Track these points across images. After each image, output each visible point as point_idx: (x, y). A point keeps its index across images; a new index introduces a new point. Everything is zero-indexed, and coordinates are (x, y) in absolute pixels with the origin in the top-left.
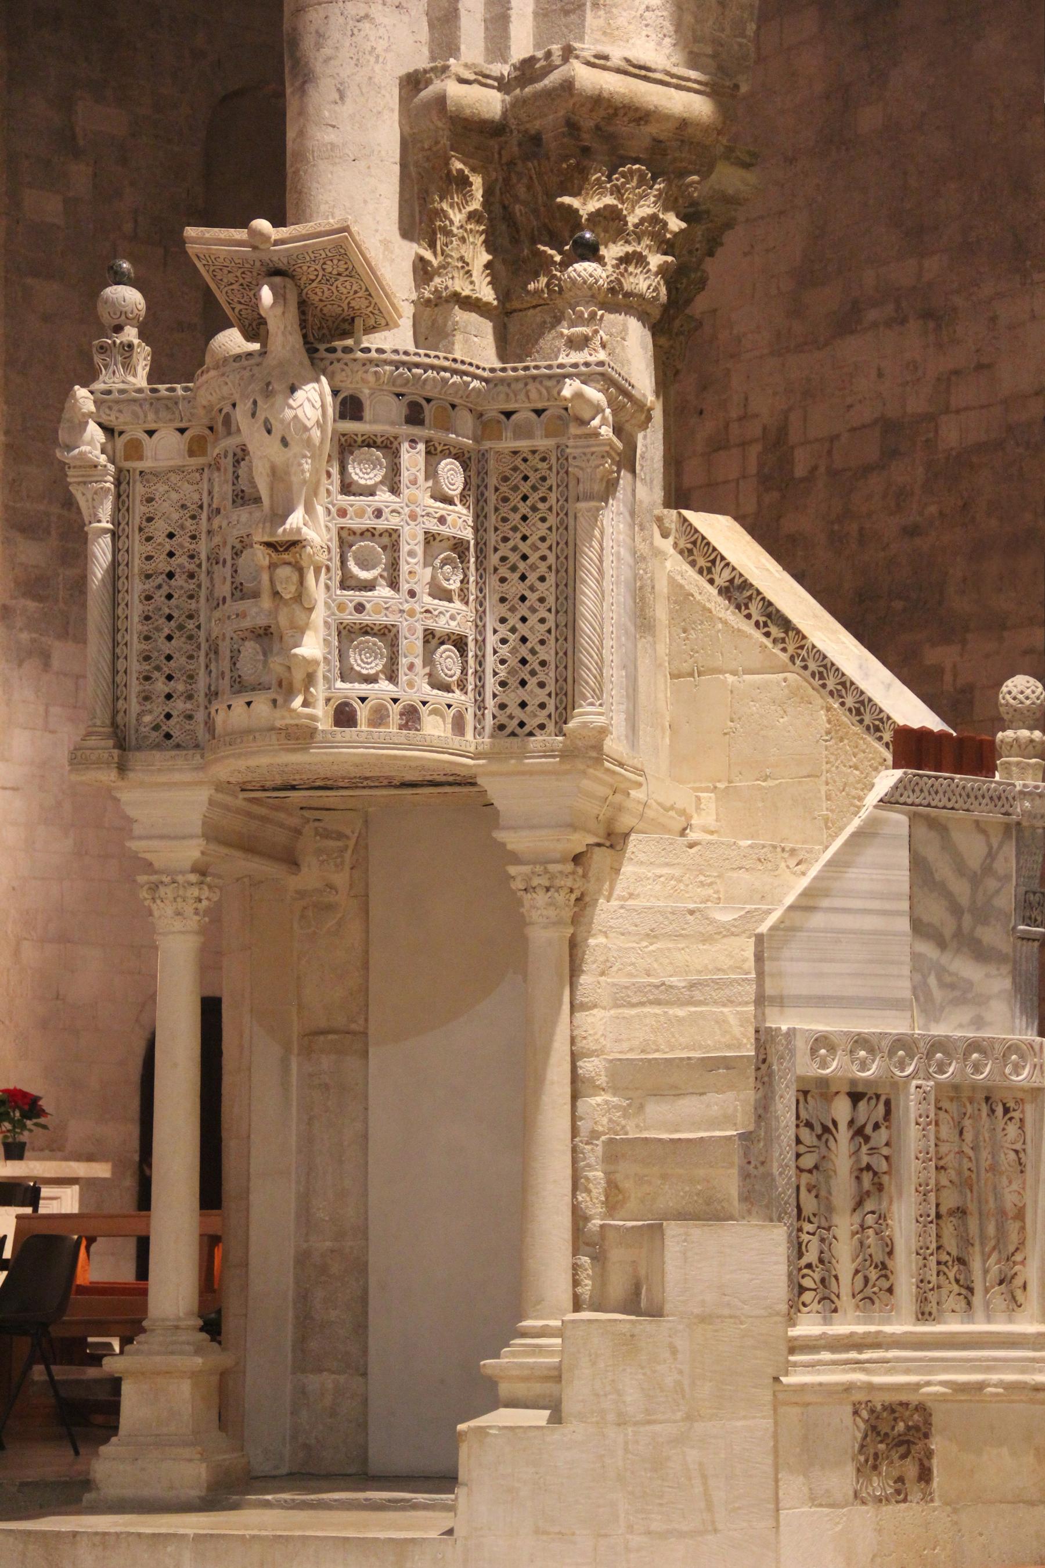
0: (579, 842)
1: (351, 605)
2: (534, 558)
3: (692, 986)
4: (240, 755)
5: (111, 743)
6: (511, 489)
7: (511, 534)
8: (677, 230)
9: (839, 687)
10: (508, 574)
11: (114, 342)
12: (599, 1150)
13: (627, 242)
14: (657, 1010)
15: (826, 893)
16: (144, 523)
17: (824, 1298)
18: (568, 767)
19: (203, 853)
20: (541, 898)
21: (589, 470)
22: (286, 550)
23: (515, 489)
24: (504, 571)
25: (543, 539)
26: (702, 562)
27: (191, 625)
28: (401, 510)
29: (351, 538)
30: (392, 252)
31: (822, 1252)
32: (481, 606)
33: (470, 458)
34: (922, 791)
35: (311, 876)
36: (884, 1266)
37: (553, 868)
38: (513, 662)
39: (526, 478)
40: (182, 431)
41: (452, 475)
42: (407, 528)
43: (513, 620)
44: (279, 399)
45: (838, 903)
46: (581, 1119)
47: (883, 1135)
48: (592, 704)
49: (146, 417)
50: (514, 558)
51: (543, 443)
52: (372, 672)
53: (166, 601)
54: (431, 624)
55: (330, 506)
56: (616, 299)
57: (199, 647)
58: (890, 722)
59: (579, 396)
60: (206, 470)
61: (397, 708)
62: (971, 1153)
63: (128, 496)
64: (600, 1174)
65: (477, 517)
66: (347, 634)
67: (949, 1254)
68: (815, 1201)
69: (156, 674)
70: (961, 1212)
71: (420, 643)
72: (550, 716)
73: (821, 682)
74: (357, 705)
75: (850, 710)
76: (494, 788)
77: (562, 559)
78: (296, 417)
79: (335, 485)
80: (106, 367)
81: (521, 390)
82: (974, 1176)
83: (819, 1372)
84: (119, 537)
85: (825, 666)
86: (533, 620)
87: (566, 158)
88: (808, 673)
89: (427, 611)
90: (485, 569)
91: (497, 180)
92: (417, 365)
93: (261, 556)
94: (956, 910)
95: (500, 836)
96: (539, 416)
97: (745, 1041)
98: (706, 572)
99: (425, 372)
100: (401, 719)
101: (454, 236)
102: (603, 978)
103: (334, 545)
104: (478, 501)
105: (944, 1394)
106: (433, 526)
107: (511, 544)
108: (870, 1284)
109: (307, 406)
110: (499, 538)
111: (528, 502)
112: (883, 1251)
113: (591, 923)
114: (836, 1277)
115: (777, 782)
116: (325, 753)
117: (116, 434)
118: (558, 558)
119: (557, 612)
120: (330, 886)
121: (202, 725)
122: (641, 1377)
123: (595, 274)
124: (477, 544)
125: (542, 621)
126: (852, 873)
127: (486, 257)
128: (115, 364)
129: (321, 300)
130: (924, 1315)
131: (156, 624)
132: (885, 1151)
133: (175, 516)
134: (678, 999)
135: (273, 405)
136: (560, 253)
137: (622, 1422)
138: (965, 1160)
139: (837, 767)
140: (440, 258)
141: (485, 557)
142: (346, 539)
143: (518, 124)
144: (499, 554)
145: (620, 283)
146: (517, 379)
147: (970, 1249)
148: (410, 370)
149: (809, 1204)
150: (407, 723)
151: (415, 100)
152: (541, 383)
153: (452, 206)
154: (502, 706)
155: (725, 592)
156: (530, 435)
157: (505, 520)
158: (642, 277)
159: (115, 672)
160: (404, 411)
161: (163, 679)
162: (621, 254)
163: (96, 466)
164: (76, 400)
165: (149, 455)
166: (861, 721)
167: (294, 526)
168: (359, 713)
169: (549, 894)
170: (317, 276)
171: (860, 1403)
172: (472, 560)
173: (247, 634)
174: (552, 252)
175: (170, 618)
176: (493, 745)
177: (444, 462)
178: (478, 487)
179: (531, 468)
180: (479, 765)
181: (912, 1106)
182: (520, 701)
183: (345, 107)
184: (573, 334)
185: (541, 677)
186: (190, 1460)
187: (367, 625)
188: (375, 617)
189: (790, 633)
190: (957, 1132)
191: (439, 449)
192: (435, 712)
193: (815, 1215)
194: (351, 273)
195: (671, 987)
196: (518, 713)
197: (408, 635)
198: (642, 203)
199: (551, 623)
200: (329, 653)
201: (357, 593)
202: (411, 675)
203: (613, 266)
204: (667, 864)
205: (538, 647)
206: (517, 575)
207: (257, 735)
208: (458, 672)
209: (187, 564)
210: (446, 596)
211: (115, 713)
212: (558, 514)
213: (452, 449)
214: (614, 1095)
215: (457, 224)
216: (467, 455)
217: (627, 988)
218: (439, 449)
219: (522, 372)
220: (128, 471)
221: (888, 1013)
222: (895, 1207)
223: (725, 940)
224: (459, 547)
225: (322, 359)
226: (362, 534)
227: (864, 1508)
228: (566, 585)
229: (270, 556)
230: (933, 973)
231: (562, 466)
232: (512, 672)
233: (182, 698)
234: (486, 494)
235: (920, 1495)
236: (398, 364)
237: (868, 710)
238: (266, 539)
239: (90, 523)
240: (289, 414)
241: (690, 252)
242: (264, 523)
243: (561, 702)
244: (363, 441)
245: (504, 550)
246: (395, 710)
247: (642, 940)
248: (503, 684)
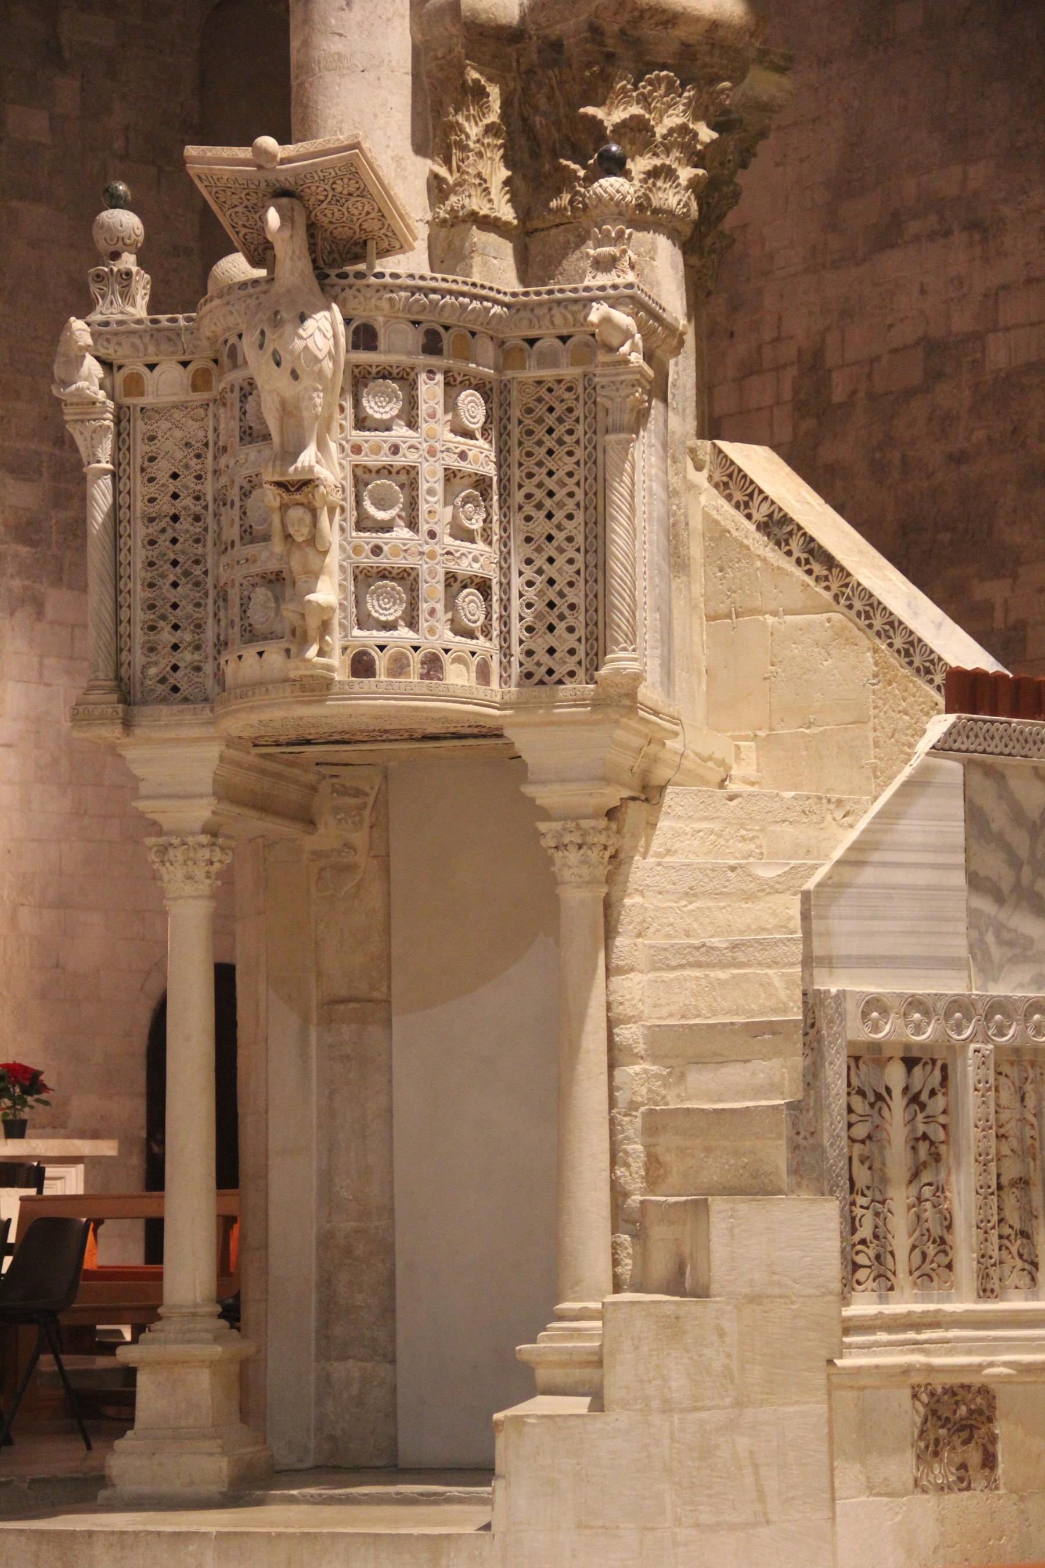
0: (612, 796)
1: (368, 548)
2: (561, 494)
3: (734, 947)
4: (252, 709)
5: (114, 697)
6: (536, 421)
7: (536, 470)
8: (708, 140)
9: (887, 627)
10: (533, 513)
11: (111, 270)
12: (638, 1122)
13: (655, 154)
14: (698, 973)
15: (876, 846)
16: (146, 463)
17: (879, 1276)
18: (601, 716)
19: (214, 813)
20: (573, 856)
21: (618, 400)
22: (298, 489)
23: (540, 421)
24: (529, 509)
25: (570, 474)
26: (738, 496)
27: (197, 571)
28: (419, 446)
29: (366, 476)
30: (404, 169)
31: (876, 1227)
32: (505, 547)
33: (491, 389)
34: (976, 736)
35: (328, 834)
36: (943, 1241)
37: (585, 824)
38: (540, 605)
39: (551, 410)
40: (185, 364)
41: (472, 407)
42: (425, 465)
43: (540, 561)
44: (288, 328)
45: (888, 856)
46: (619, 1089)
47: (940, 1101)
48: (625, 649)
49: (146, 349)
50: (539, 494)
51: (569, 372)
52: (391, 618)
53: (171, 546)
54: (452, 566)
55: (344, 443)
56: (644, 216)
57: (206, 594)
58: (942, 663)
59: (606, 320)
60: (211, 405)
62: (1033, 1120)
63: (129, 435)
64: (639, 1147)
65: (499, 451)
66: (364, 579)
67: (1011, 1227)
68: (868, 1172)
69: (161, 624)
70: (1023, 1183)
71: (441, 587)
72: (580, 663)
73: (867, 622)
74: (375, 653)
75: (898, 651)
76: (522, 740)
77: (591, 495)
78: (306, 347)
79: (349, 422)
80: (103, 297)
82: (1037, 1145)
83: (875, 1354)
84: (120, 478)
85: (871, 605)
86: (561, 560)
87: (589, 65)
88: (853, 612)
89: (448, 553)
90: (509, 508)
91: (515, 90)
92: (434, 291)
93: (272, 497)
94: (1015, 863)
95: (529, 790)
96: (564, 343)
97: (791, 1004)
98: (743, 506)
99: (443, 297)
100: (423, 668)
101: (470, 151)
102: (640, 940)
103: (349, 484)
104: (501, 434)
105: (1008, 1375)
106: (455, 463)
107: (536, 480)
108: (928, 1260)
109: (317, 334)
110: (524, 474)
111: (554, 435)
112: (941, 1225)
113: (627, 881)
114: (892, 1253)
115: (822, 729)
116: (343, 706)
117: (115, 369)
118: (586, 494)
119: (586, 552)
120: (349, 846)
121: (211, 676)
122: (687, 1361)
123: (622, 189)
124: (500, 481)
125: (571, 561)
126: (903, 825)
127: (505, 173)
128: (113, 293)
129: (331, 222)
130: (986, 1292)
131: (161, 570)
132: (942, 1119)
133: (179, 455)
134: (720, 961)
135: (281, 336)
136: (584, 166)
137: (668, 1408)
138: (1028, 1128)
139: (885, 713)
140: (456, 175)
141: (509, 495)
142: (361, 477)
143: (537, 29)
144: (523, 491)
145: (648, 199)
146: (541, 304)
147: (1034, 1222)
148: (426, 296)
149: (862, 1176)
150: (429, 672)
151: (427, 5)
152: (566, 307)
153: (468, 119)
154: (529, 653)
155: (764, 527)
156: (556, 365)
157: (529, 454)
158: (671, 192)
159: (118, 622)
160: (421, 340)
161: (168, 628)
162: (649, 168)
163: (94, 403)
164: (72, 333)
165: (150, 389)
166: (910, 663)
167: (306, 464)
168: (377, 662)
169: (582, 852)
170: (326, 196)
171: (919, 1386)
172: (496, 498)
173: (257, 579)
174: (574, 166)
175: (175, 563)
176: (520, 693)
177: (463, 394)
178: (501, 419)
179: (557, 398)
180: (506, 716)
181: (970, 1072)
182: (547, 648)
183: (352, 14)
184: (599, 255)
185: (570, 621)
186: (211, 1454)
187: (385, 569)
188: (394, 560)
189: (834, 570)
190: (1018, 1097)
191: (459, 379)
192: (459, 660)
193: (868, 1188)
194: (363, 193)
195: (712, 948)
196: (546, 659)
197: (428, 579)
198: (670, 112)
199: (580, 564)
200: (345, 599)
201: (374, 535)
202: (432, 622)
203: (640, 181)
204: (706, 818)
205: (567, 590)
206: (542, 514)
207: (270, 687)
208: (482, 617)
209: (192, 506)
210: (469, 536)
211: (118, 665)
212: (586, 448)
213: (472, 379)
214: (654, 1064)
215: (473, 138)
216: (488, 386)
217: (665, 950)
218: (459, 379)
219: (546, 297)
220: (129, 408)
221: (943, 973)
222: (953, 1178)
223: (769, 898)
224: (481, 483)
225: (333, 286)
226: (378, 472)
227: (925, 1496)
228: (595, 523)
229: (281, 497)
230: (991, 929)
231: (589, 396)
232: (539, 616)
233: (190, 649)
234: (510, 427)
235: (984, 1483)
236: (414, 290)
237: (918, 651)
238: (276, 478)
239: (89, 463)
240: (298, 344)
241: (722, 164)
242: (274, 462)
243: (592, 648)
244: (378, 373)
245: (529, 486)
246: (416, 658)
247: (680, 899)
248: (530, 629)
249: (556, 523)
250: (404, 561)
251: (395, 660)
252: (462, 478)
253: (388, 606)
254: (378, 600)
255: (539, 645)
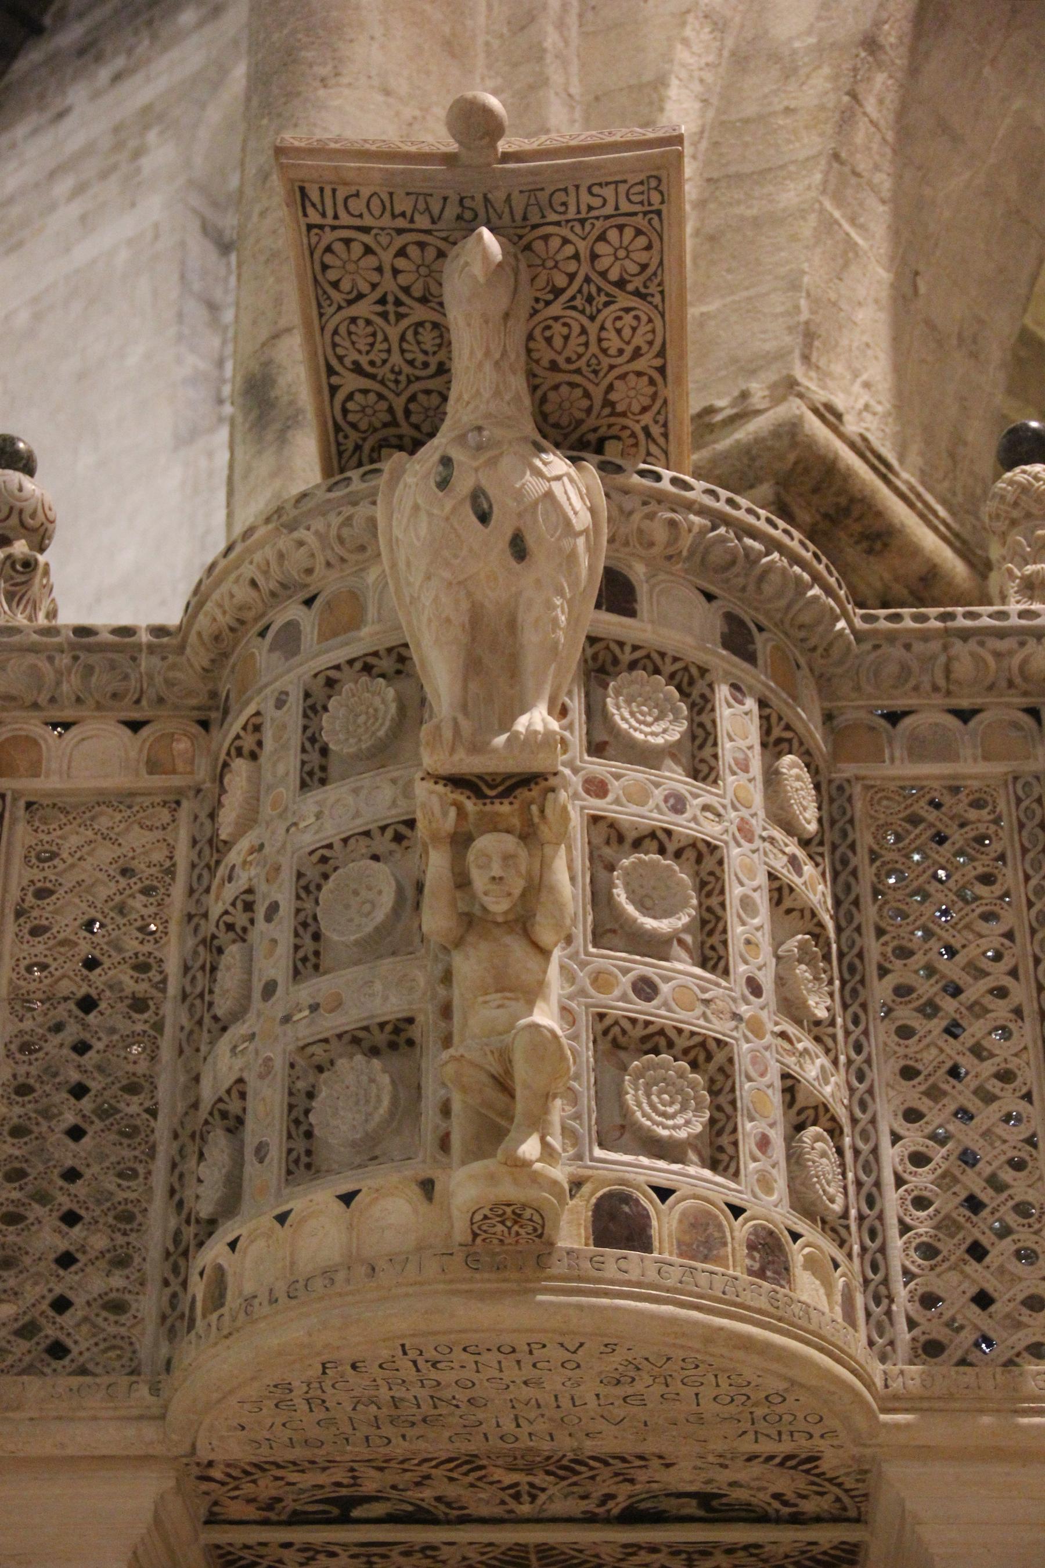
1: (626, 981)
2: (975, 990)
10: (916, 1022)
24: (905, 1014)
29: (608, 852)
38: (946, 1203)
42: (735, 851)
51: (972, 768)
61: (740, 1230)
74: (649, 1202)
78: (549, 495)
81: (933, 657)
89: (783, 1035)
90: (864, 1006)
110: (889, 949)
116: (580, 1307)
124: (841, 955)
154: (929, 1301)
156: (947, 752)
160: (719, 625)
168: (655, 1223)
177: (788, 759)
180: (897, 1426)
187: (662, 1032)
188: (683, 1015)
191: (777, 732)
197: (753, 1074)
205: (1007, 1175)
206: (937, 1025)
234: (854, 861)
249: (970, 1042)
250: (702, 1022)
251: (693, 1226)
252: (789, 911)
253: (670, 1110)
254: (648, 1095)
255: (954, 1286)
